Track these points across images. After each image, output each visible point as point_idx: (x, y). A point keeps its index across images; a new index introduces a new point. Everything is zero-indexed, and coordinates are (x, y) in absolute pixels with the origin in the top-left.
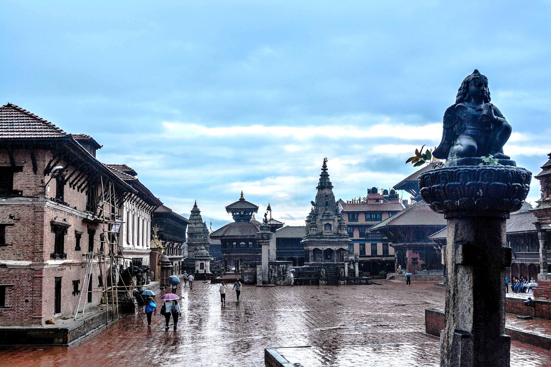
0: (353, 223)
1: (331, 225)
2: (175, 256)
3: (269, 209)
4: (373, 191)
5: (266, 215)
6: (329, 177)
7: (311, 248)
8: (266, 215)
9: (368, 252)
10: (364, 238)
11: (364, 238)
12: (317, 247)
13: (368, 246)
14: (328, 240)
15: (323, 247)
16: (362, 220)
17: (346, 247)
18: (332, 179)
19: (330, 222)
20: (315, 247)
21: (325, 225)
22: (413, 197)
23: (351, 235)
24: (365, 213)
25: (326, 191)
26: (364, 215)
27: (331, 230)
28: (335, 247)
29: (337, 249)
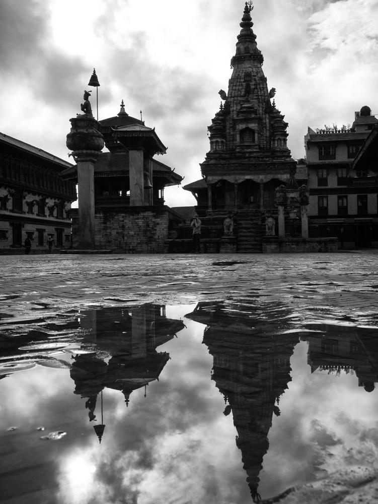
0: (327, 161)
1: (252, 132)
2: (35, 216)
3: (94, 81)
5: (87, 95)
6: (256, 40)
8: (87, 95)
9: (353, 209)
10: (345, 187)
11: (345, 187)
12: (225, 178)
15: (237, 177)
18: (262, 43)
19: (253, 126)
20: (220, 178)
21: (242, 132)
23: (323, 181)
25: (247, 66)
26: (346, 149)
27: (254, 141)
28: (261, 177)
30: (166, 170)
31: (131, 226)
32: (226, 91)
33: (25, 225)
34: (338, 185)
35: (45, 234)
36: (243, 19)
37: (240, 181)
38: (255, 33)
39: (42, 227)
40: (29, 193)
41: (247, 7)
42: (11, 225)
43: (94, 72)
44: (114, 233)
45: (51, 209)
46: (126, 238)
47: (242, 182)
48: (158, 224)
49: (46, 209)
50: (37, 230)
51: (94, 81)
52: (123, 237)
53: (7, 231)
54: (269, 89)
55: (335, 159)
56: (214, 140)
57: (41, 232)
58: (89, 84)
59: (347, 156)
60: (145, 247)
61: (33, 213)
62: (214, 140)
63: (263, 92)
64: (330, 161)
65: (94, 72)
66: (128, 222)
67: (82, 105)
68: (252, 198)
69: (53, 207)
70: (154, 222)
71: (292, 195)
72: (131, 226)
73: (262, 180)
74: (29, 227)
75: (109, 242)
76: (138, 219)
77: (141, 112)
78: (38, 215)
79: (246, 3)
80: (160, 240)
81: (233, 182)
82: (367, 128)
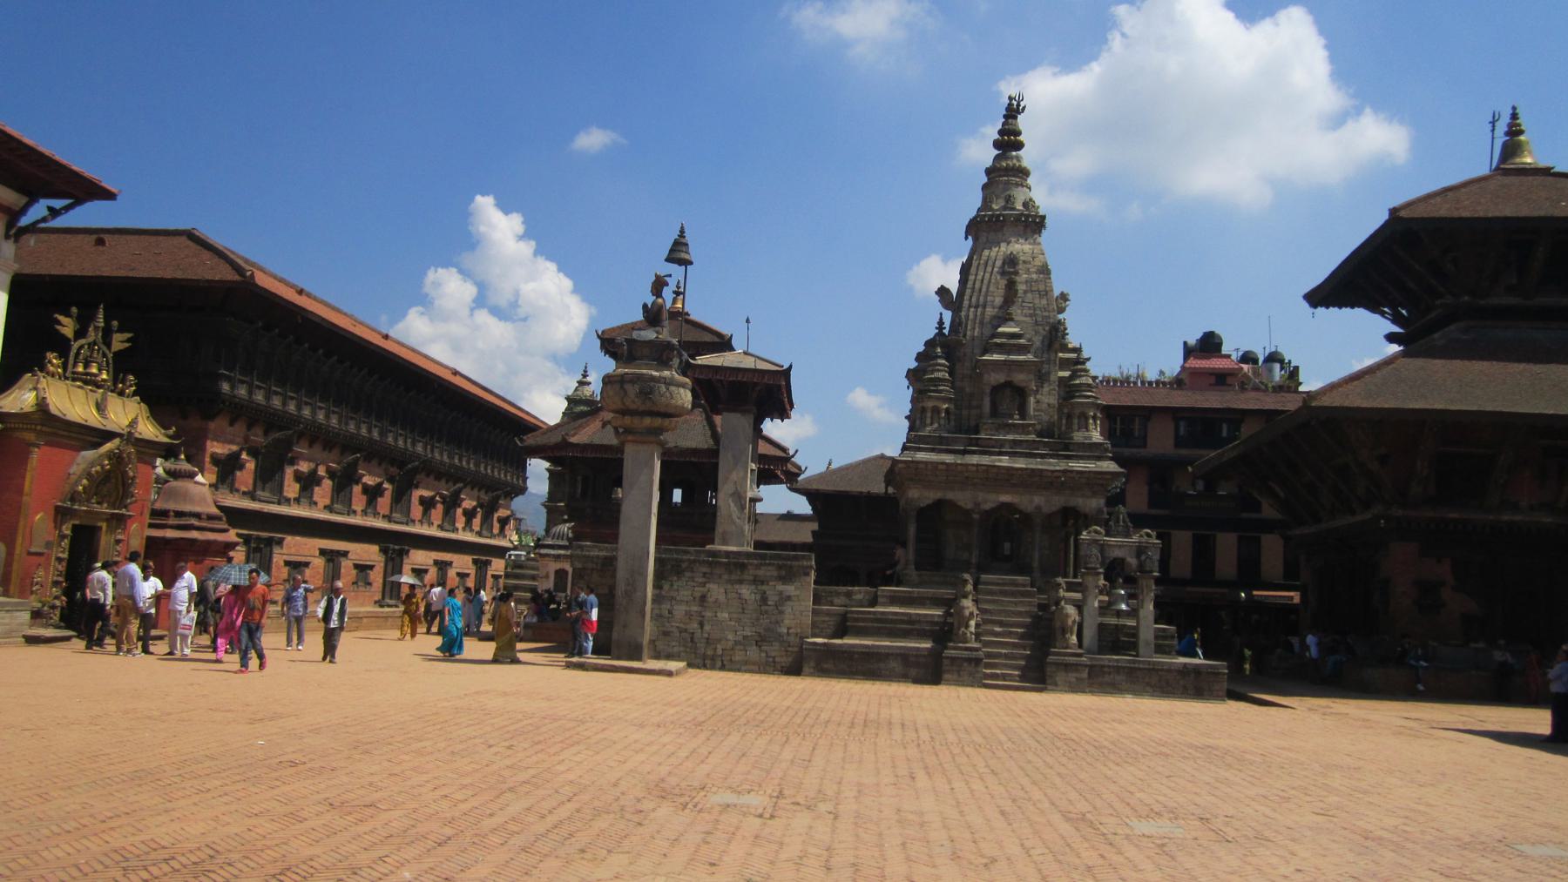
0: (1127, 452)
2: (433, 532)
3: (678, 253)
4: (1209, 344)
5: (659, 285)
6: (1030, 181)
7: (920, 496)
12: (950, 495)
13: (1183, 539)
14: (1004, 461)
15: (981, 496)
16: (1161, 441)
17: (1094, 503)
19: (1019, 378)
20: (939, 495)
21: (997, 389)
22: (1397, 329)
24: (1175, 413)
28: (1038, 500)
29: (1046, 510)
30: (780, 454)
31: (722, 598)
32: (954, 287)
33: (413, 552)
34: (1151, 504)
35: (452, 573)
36: (1001, 132)
37: (987, 506)
38: (1025, 163)
39: (446, 556)
40: (428, 476)
41: (1010, 105)
42: (384, 551)
43: (682, 231)
44: (680, 610)
45: (470, 515)
46: (707, 628)
47: (993, 510)
48: (789, 598)
49: (459, 511)
50: (436, 562)
51: (678, 253)
52: (701, 625)
53: (371, 567)
54: (1056, 293)
55: (1145, 446)
56: (930, 404)
57: (442, 566)
58: (667, 260)
59: (1171, 442)
60: (753, 653)
61: (430, 524)
62: (930, 404)
63: (1044, 302)
64: (1134, 450)
65: (682, 231)
66: (716, 591)
67: (645, 306)
68: (1007, 546)
69: (475, 508)
70: (781, 593)
71: (1118, 553)
72: (722, 598)
73: (1038, 508)
74: (420, 557)
75: (666, 634)
76: (741, 582)
77: (748, 321)
78: (441, 527)
79: (1010, 98)
80: (792, 639)
81: (969, 506)
82: (1212, 380)
